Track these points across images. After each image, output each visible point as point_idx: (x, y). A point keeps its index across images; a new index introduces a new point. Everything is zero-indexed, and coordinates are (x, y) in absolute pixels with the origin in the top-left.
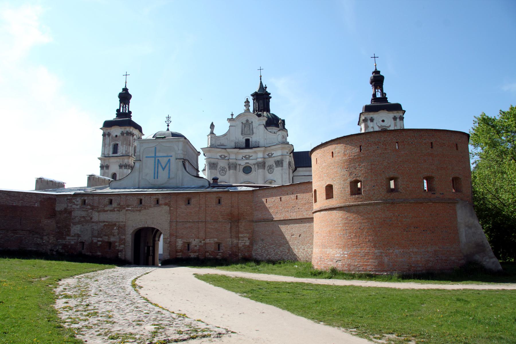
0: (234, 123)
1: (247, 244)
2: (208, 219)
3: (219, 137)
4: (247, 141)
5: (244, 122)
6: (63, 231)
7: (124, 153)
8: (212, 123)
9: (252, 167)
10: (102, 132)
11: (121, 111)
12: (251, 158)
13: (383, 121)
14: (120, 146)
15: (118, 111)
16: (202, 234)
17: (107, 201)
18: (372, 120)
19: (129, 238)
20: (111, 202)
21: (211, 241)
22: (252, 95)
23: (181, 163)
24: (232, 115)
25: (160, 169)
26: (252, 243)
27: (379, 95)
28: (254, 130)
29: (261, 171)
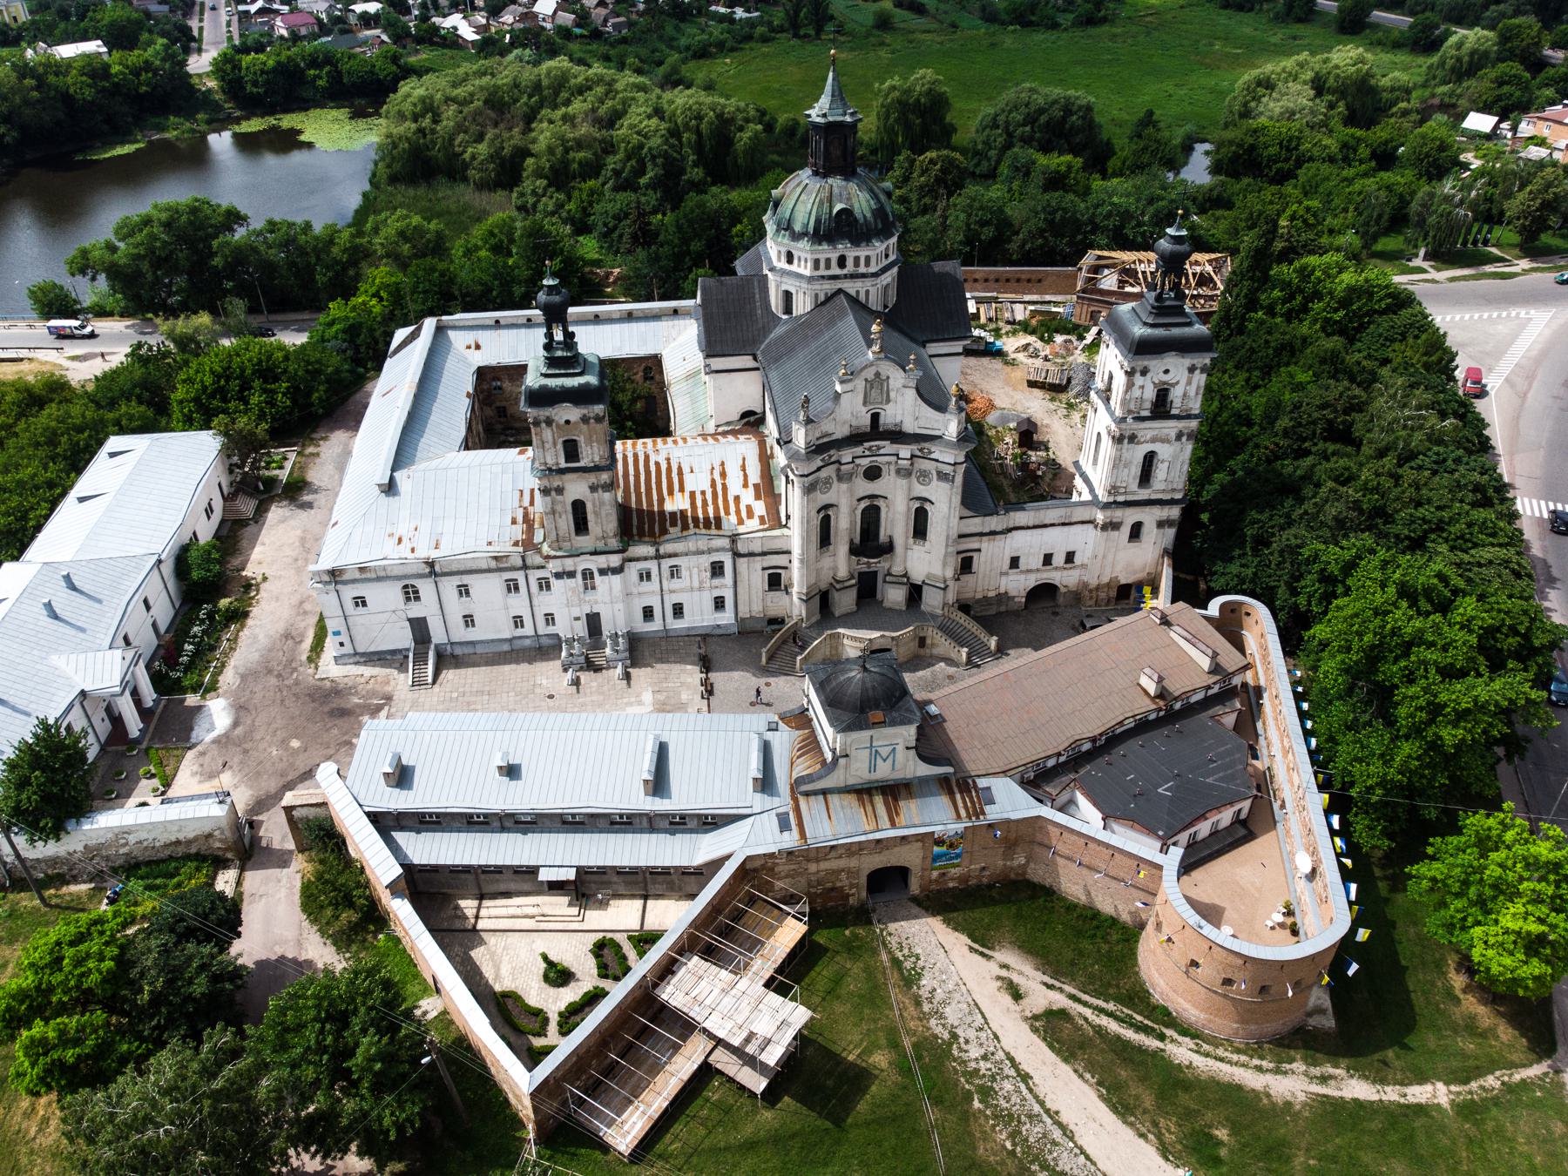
4: (875, 417)
7: (597, 459)
13: (1166, 372)
25: (879, 761)
28: (892, 395)
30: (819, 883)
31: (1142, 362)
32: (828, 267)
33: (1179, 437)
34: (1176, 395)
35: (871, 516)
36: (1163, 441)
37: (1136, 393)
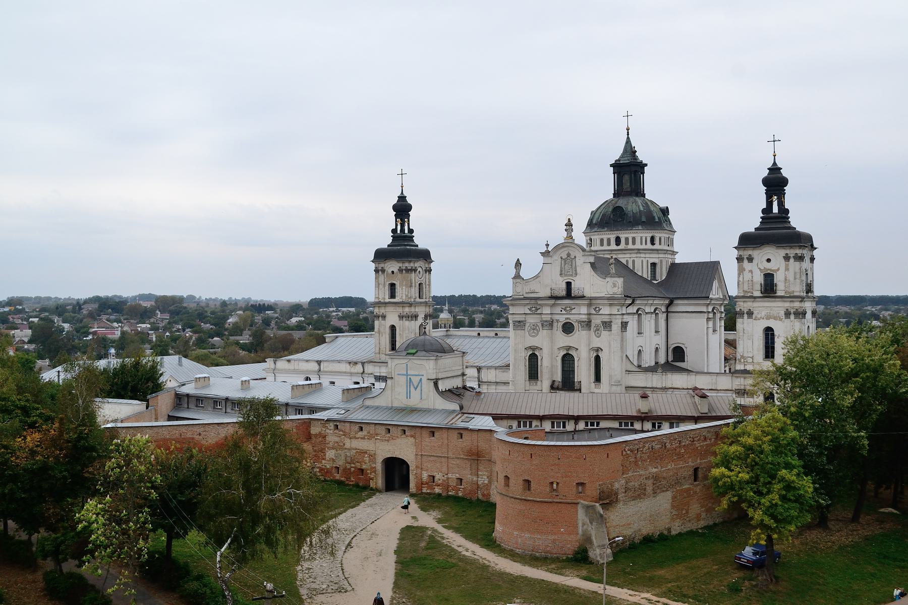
0: (548, 260)
1: (486, 482)
2: (450, 455)
3: (527, 281)
4: (569, 284)
5: (565, 256)
6: (319, 454)
8: (518, 260)
9: (576, 325)
10: (373, 266)
12: (573, 312)
13: (769, 260)
14: (397, 287)
16: (445, 469)
17: (357, 428)
18: (750, 259)
19: (379, 467)
20: (361, 429)
21: (453, 476)
22: (611, 165)
23: (432, 384)
24: (547, 245)
25: (412, 389)
26: (490, 482)
27: (775, 209)
28: (578, 269)
29: (584, 333)
30: (352, 462)
31: (746, 253)
32: (609, 244)
33: (788, 314)
34: (779, 279)
35: (568, 361)
36: (775, 318)
37: (747, 276)
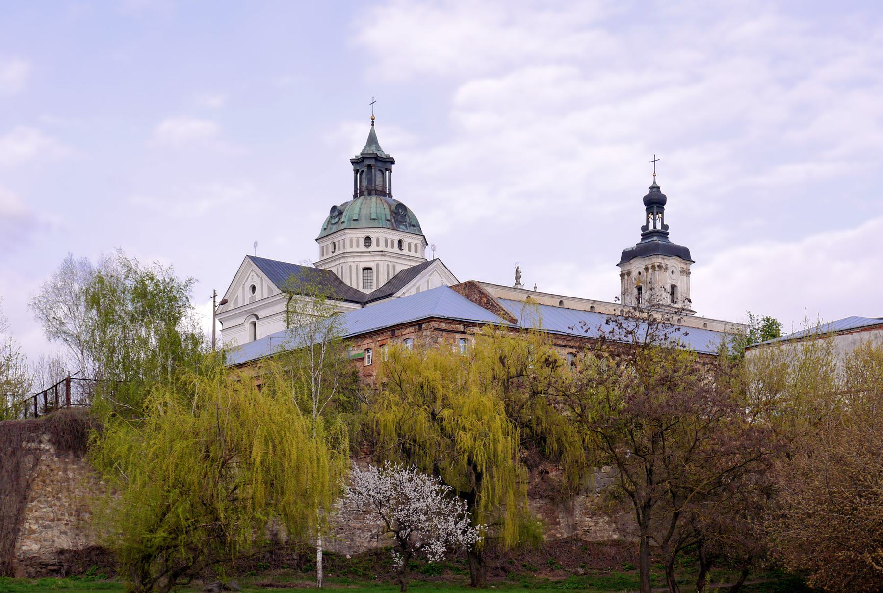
10: (618, 270)
11: (651, 228)
15: (645, 228)
